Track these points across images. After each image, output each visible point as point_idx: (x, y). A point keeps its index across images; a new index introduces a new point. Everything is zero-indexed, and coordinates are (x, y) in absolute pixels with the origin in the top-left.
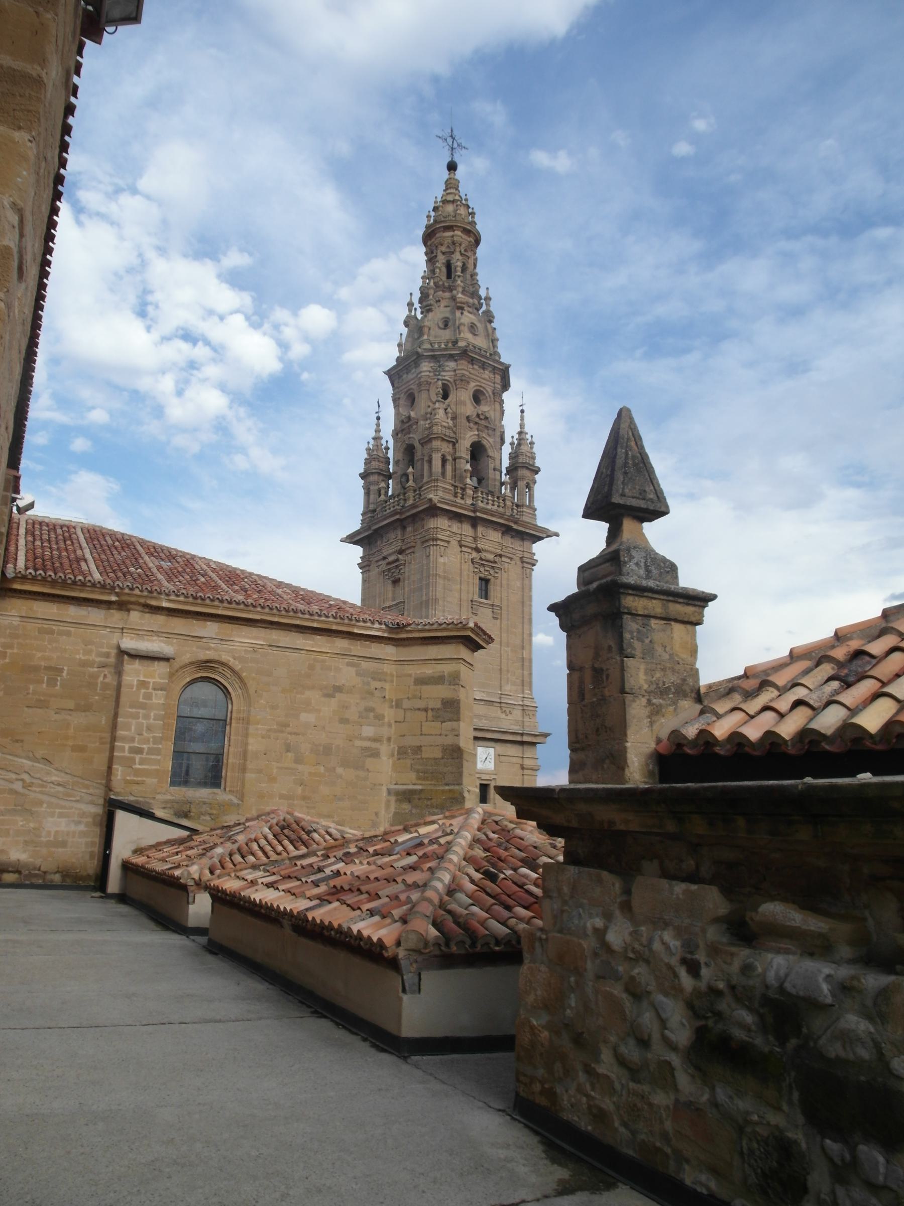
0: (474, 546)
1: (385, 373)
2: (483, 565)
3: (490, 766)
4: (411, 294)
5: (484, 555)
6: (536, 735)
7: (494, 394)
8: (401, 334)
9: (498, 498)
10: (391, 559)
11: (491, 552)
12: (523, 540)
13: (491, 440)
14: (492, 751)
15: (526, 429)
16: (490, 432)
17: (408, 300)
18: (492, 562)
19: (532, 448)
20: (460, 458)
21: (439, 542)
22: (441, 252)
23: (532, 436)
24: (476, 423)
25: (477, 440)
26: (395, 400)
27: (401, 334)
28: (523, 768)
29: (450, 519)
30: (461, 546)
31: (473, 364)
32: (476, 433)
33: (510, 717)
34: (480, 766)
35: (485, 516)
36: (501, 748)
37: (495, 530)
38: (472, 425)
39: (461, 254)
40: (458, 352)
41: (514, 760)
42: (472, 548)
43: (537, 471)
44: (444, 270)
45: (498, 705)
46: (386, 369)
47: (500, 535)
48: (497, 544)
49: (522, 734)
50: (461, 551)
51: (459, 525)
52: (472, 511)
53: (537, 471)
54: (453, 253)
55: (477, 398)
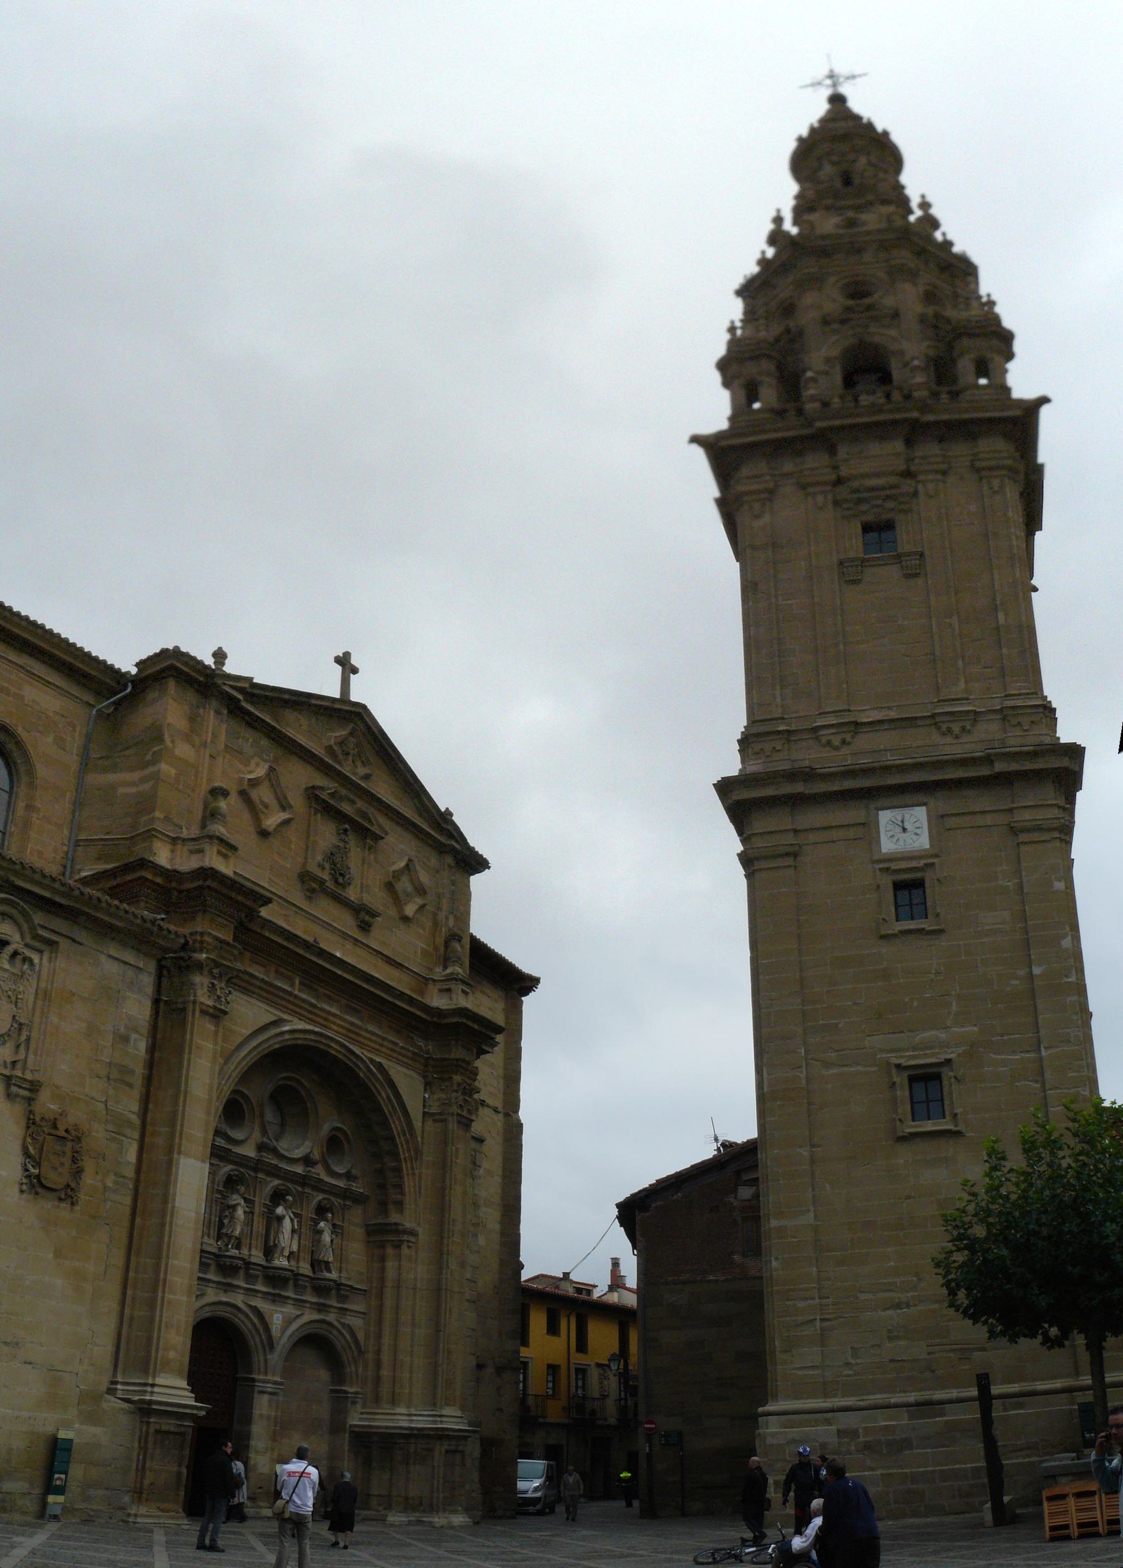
3: (923, 842)
34: (887, 846)
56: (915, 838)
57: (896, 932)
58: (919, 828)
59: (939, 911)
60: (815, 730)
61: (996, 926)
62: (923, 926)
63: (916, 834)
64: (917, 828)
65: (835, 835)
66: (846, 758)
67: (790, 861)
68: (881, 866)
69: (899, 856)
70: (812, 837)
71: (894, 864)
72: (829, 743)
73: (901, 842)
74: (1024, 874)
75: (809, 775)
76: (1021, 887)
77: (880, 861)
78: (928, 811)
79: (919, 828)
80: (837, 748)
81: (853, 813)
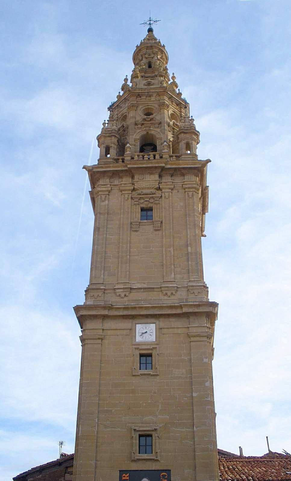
3: (153, 338)
5: (139, 192)
6: (199, 306)
11: (148, 188)
12: (183, 175)
13: (158, 130)
14: (153, 326)
18: (150, 194)
21: (100, 193)
25: (145, 133)
28: (189, 336)
29: (111, 177)
30: (121, 191)
31: (140, 97)
33: (172, 297)
34: (138, 339)
35: (135, 166)
36: (163, 323)
37: (151, 174)
38: (139, 126)
39: (146, 58)
41: (179, 331)
45: (160, 290)
47: (157, 177)
48: (154, 182)
49: (181, 307)
50: (122, 194)
51: (120, 180)
56: (150, 336)
57: (139, 374)
58: (152, 332)
59: (157, 367)
60: (115, 289)
61: (179, 375)
62: (150, 373)
63: (150, 335)
64: (151, 332)
65: (118, 332)
66: (125, 302)
67: (100, 341)
68: (135, 347)
69: (144, 343)
70: (109, 332)
71: (141, 346)
72: (120, 295)
73: (144, 338)
74: (192, 354)
75: (111, 308)
76: (190, 360)
77: (134, 345)
78: (156, 326)
79: (152, 332)
80: (122, 298)
81: (126, 324)
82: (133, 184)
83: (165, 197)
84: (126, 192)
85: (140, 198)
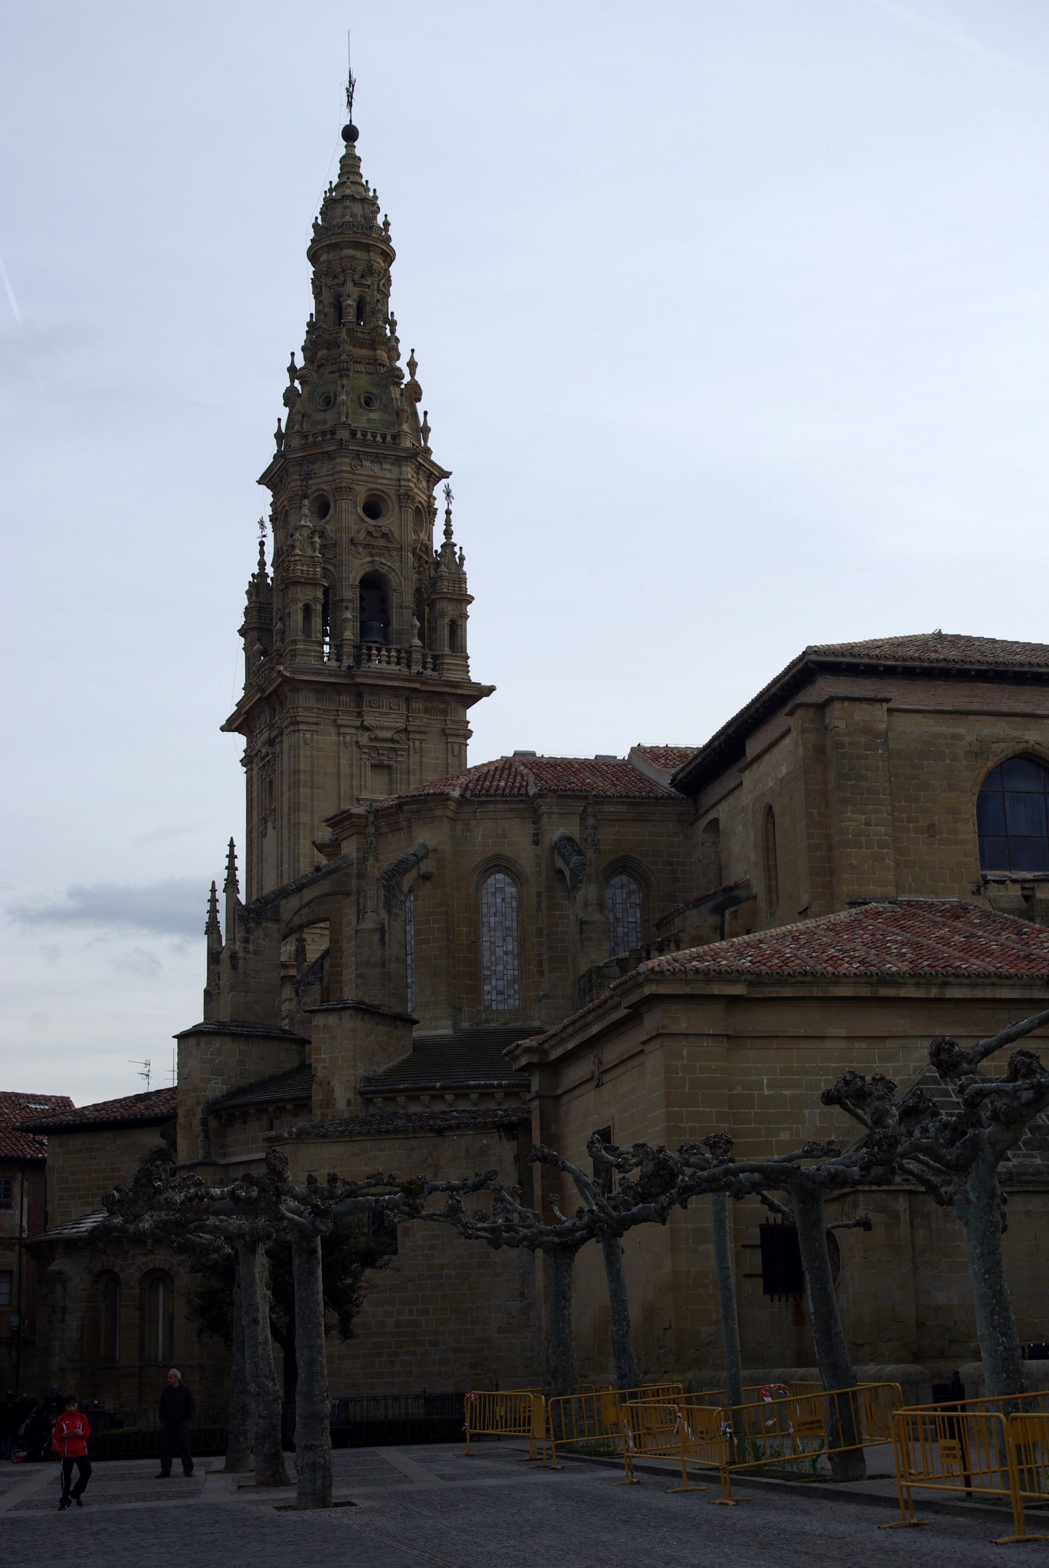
0: (358, 723)
1: (259, 482)
2: (377, 749)
4: (293, 354)
7: (399, 496)
8: (279, 420)
9: (398, 651)
10: (264, 751)
11: (388, 729)
15: (454, 540)
16: (394, 553)
17: (289, 365)
19: (461, 564)
20: (342, 601)
21: (302, 727)
22: (326, 285)
23: (461, 548)
24: (366, 546)
25: (368, 568)
26: (272, 519)
27: (279, 420)
30: (339, 726)
32: (369, 559)
39: (355, 285)
40: (334, 448)
42: (357, 728)
43: (470, 600)
44: (330, 311)
46: (258, 479)
52: (345, 676)
53: (470, 600)
54: (343, 284)
55: (373, 509)
82: (360, 714)
83: (414, 749)
84: (349, 731)
85: (372, 746)
